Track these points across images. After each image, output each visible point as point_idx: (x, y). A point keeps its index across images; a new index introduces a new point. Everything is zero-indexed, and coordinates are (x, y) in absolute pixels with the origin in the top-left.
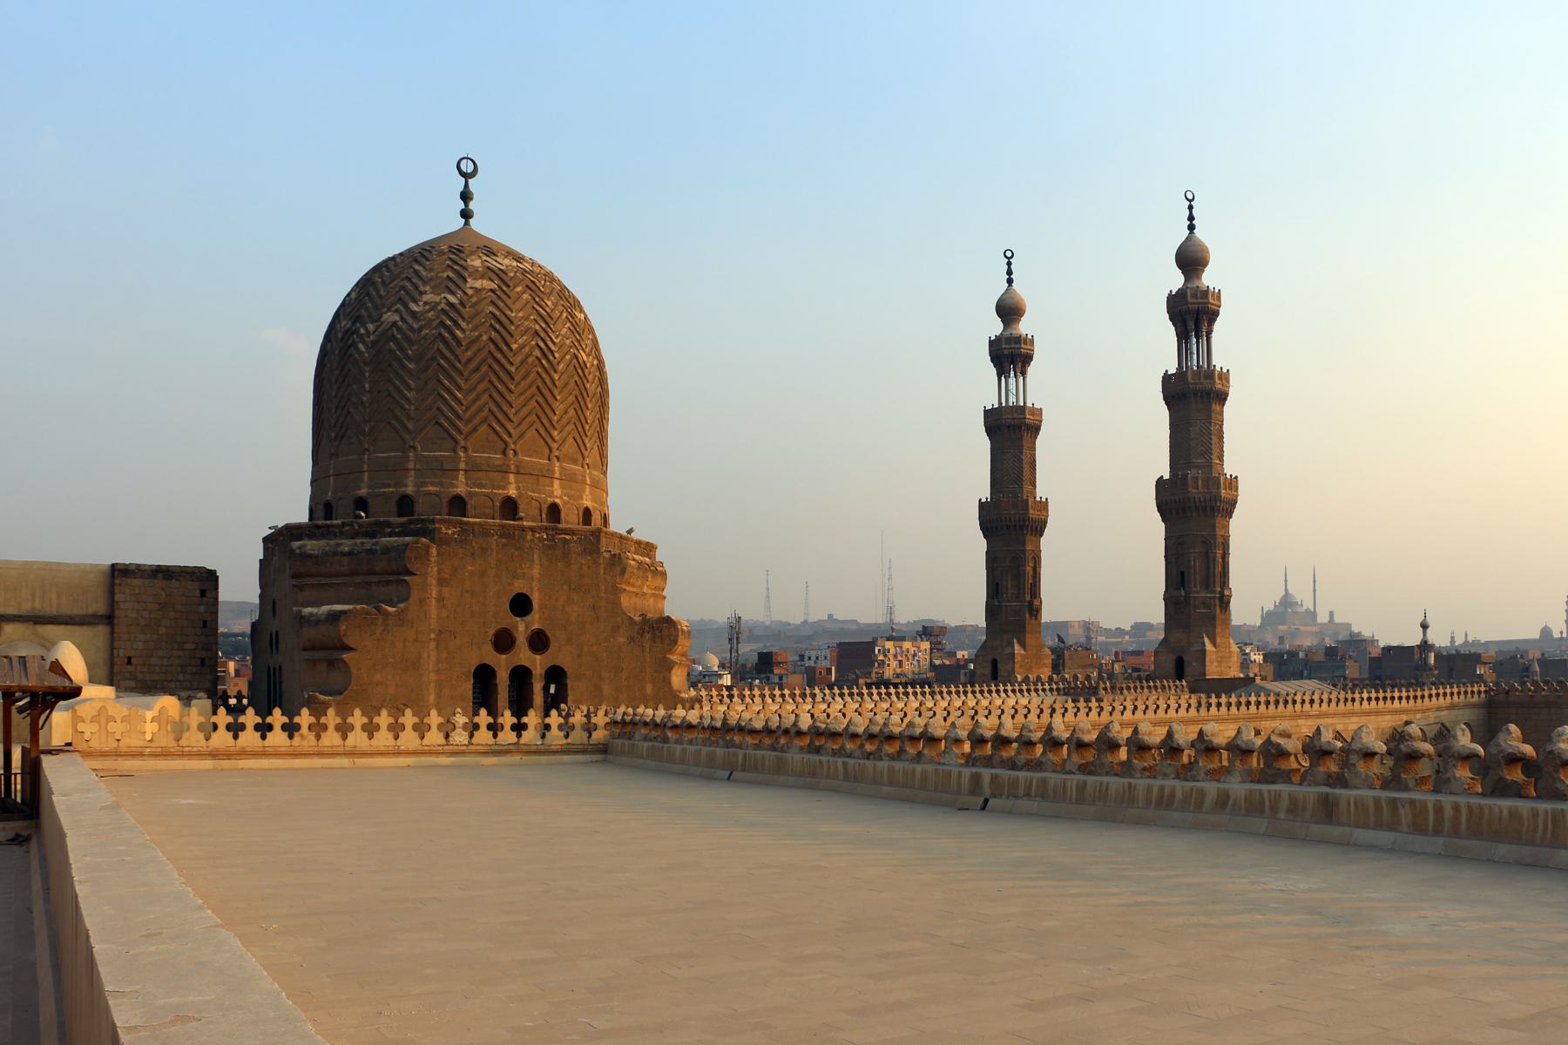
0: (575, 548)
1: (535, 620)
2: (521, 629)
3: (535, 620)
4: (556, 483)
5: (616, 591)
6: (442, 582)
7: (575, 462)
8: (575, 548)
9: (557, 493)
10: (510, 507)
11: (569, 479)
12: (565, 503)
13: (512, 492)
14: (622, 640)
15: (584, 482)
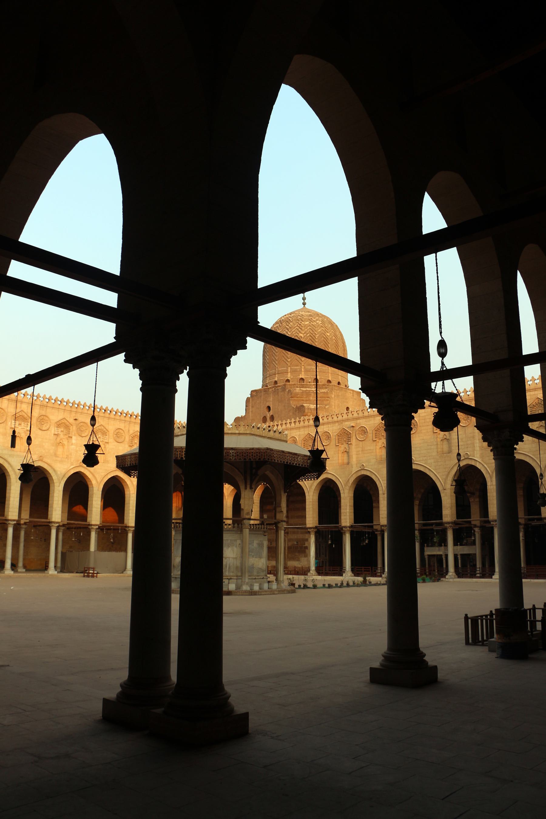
0: (280, 390)
1: (271, 413)
2: (268, 416)
3: (271, 413)
4: (289, 374)
5: (289, 400)
6: (252, 407)
7: (297, 366)
8: (280, 390)
9: (289, 376)
10: (276, 382)
11: (293, 371)
12: (291, 379)
13: (276, 379)
14: (291, 414)
15: (301, 371)
